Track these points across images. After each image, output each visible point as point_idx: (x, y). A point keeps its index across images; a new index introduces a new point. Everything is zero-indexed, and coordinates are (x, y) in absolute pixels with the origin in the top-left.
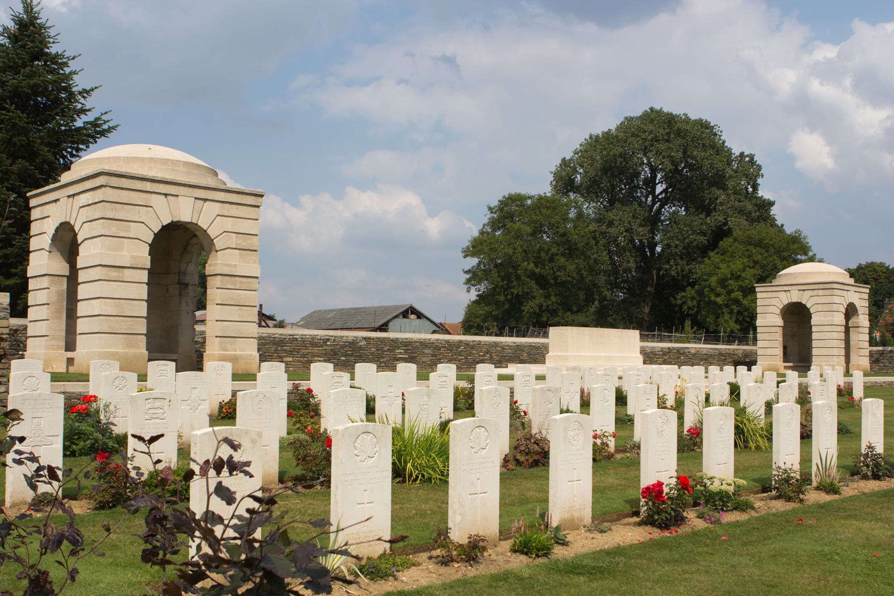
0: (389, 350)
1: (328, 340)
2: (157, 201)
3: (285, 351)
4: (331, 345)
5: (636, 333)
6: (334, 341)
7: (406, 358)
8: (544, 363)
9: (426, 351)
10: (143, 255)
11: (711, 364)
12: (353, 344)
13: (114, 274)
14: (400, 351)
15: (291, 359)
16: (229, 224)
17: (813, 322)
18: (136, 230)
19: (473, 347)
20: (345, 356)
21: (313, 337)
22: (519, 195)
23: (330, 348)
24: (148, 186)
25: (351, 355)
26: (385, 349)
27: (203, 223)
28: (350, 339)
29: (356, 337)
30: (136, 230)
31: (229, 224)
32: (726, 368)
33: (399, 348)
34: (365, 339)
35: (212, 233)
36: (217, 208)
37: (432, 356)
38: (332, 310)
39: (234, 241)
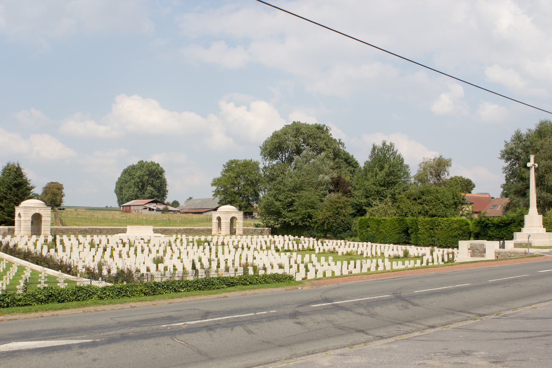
2: (33, 210)
5: (152, 226)
8: (126, 233)
10: (30, 219)
12: (85, 229)
13: (26, 222)
16: (45, 213)
17: (221, 222)
18: (29, 215)
19: (118, 229)
22: (235, 160)
24: (31, 208)
27: (40, 213)
30: (29, 215)
31: (45, 213)
35: (42, 214)
36: (43, 210)
38: (199, 199)
39: (46, 215)
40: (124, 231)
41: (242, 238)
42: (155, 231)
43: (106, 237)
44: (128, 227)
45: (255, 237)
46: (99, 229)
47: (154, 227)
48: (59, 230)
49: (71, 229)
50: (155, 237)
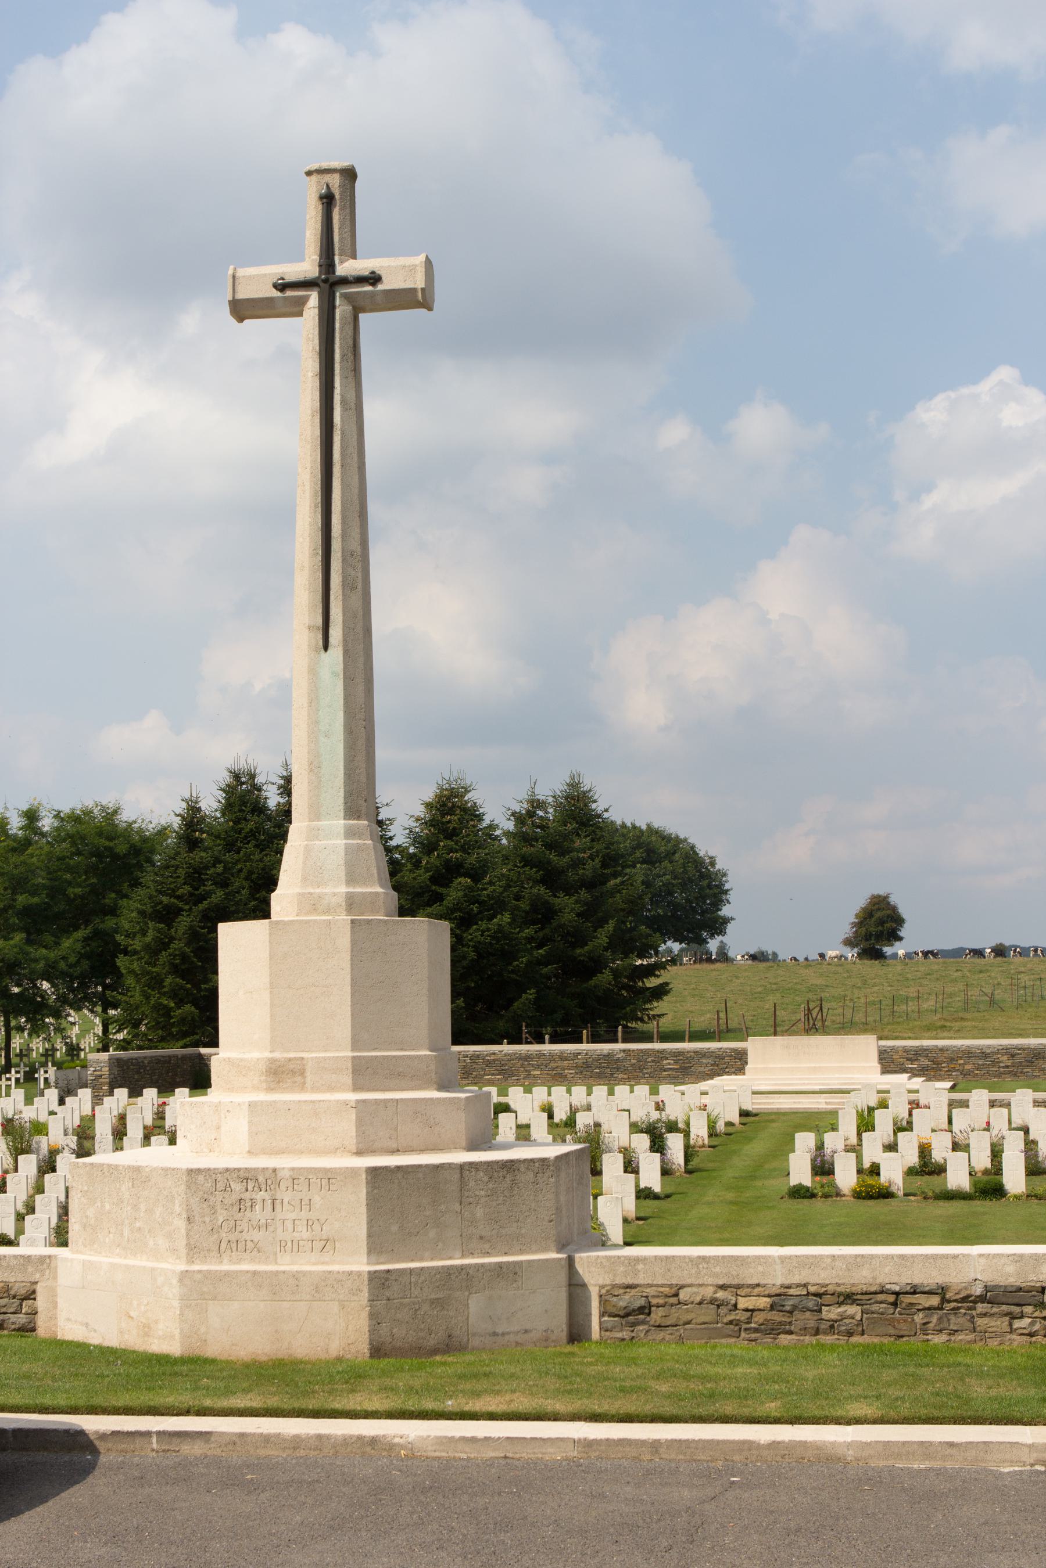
0: (653, 1061)
1: (579, 1054)
3: (532, 1066)
4: (582, 1059)
6: (587, 1054)
7: (677, 1069)
9: (704, 1061)
11: (638, 1083)
14: (668, 1061)
15: (539, 1073)
20: (599, 1068)
21: (562, 1052)
23: (581, 1061)
25: (607, 1067)
26: (649, 1060)
28: (605, 1052)
29: (613, 1050)
32: (618, 1089)
33: (667, 1058)
34: (624, 1051)
37: (712, 1065)
40: (737, 1063)
41: (964, 1104)
42: (889, 1063)
43: (654, 1092)
44: (754, 1046)
45: (980, 1097)
46: (677, 1054)
47: (883, 1043)
48: (489, 1063)
49: (540, 1055)
50: (754, 1093)
